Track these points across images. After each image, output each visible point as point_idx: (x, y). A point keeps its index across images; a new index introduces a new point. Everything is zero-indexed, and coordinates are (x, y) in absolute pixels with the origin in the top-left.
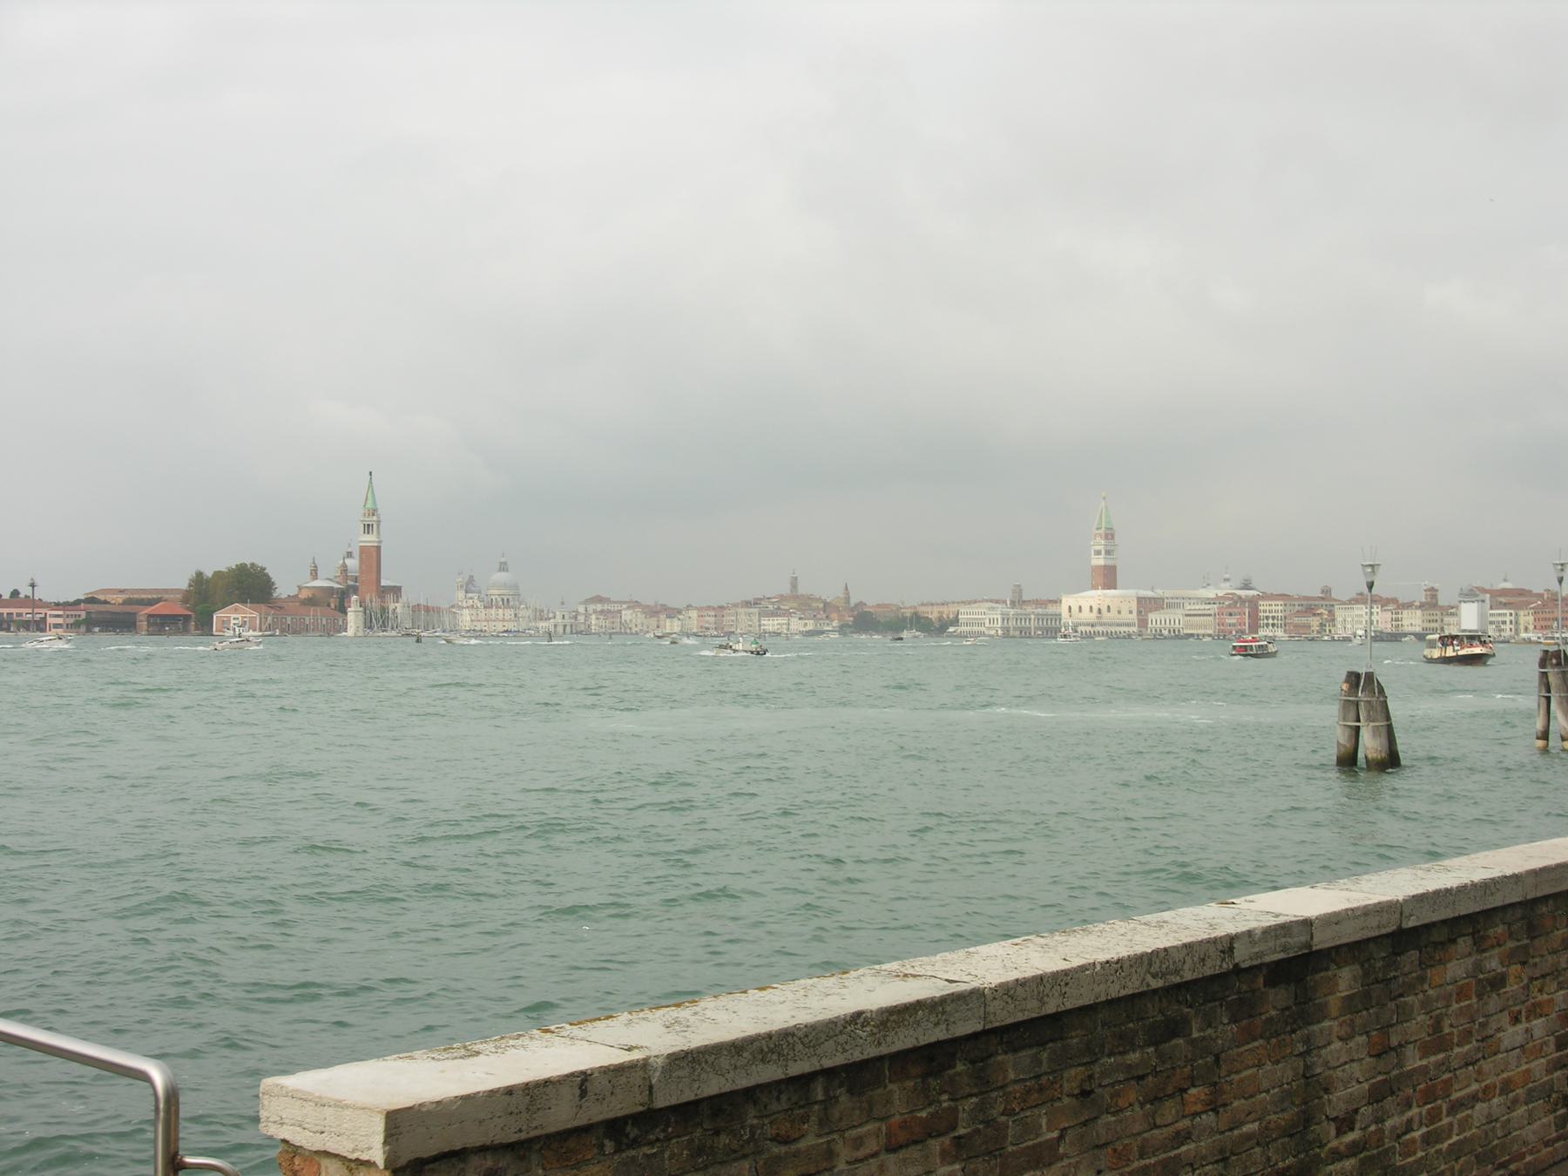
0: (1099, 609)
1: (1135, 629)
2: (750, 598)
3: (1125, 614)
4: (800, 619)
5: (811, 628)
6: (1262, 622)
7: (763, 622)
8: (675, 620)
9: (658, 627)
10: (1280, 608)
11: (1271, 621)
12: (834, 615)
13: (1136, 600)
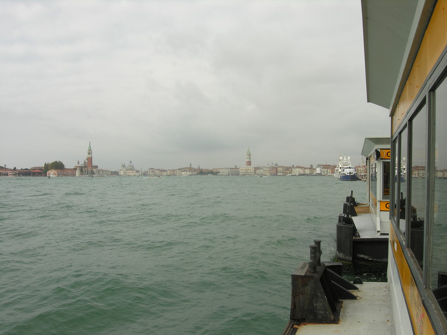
1: (254, 174)
2: (180, 168)
3: (252, 170)
4: (189, 172)
5: (191, 174)
7: (182, 173)
8: (165, 172)
9: (162, 174)
10: (282, 169)
11: (280, 172)
12: (196, 171)
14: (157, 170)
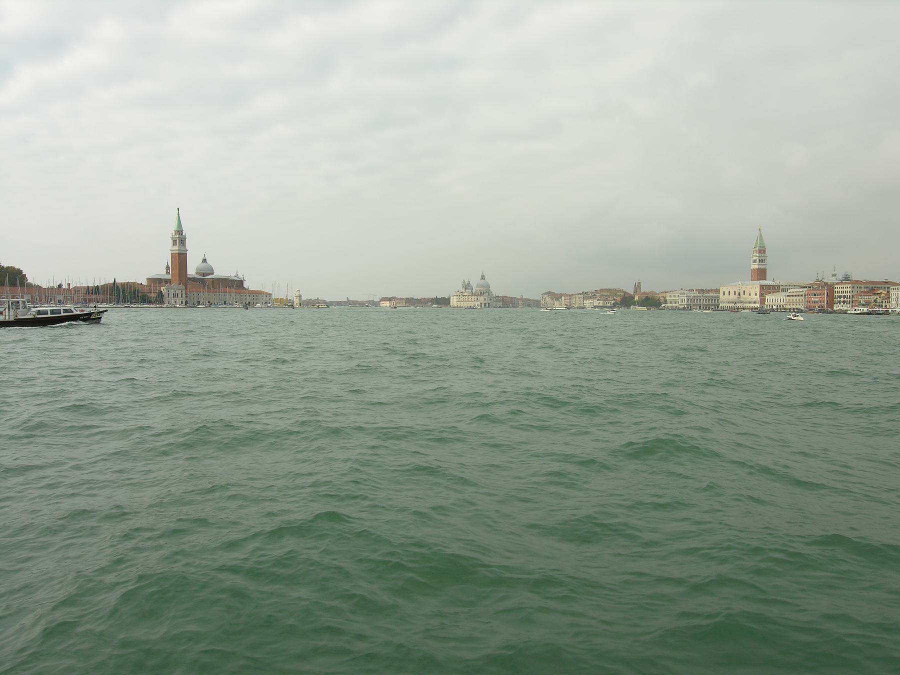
0: (739, 293)
3: (753, 296)
4: (598, 300)
6: (836, 300)
7: (585, 302)
10: (849, 290)
11: (842, 299)
13: (759, 286)
14: (586, 295)
